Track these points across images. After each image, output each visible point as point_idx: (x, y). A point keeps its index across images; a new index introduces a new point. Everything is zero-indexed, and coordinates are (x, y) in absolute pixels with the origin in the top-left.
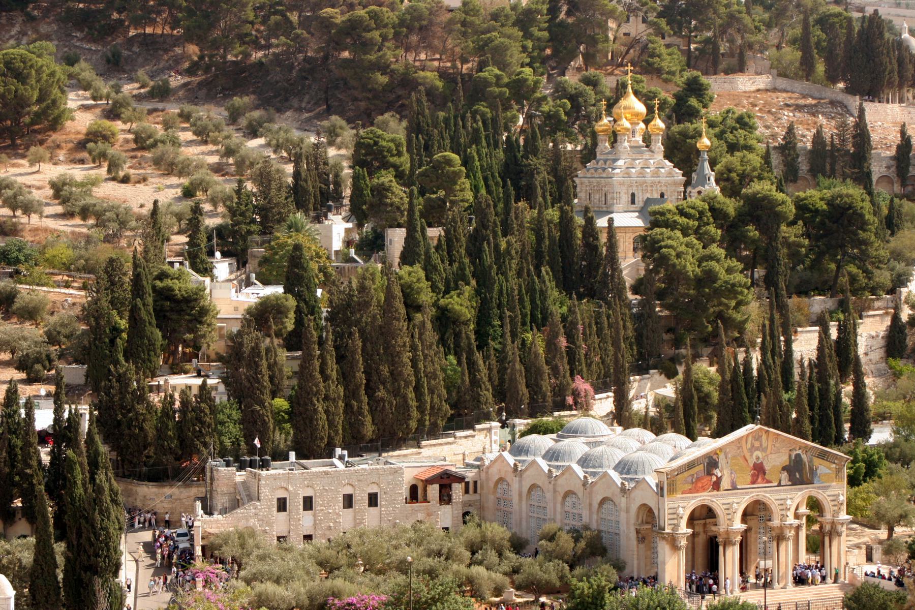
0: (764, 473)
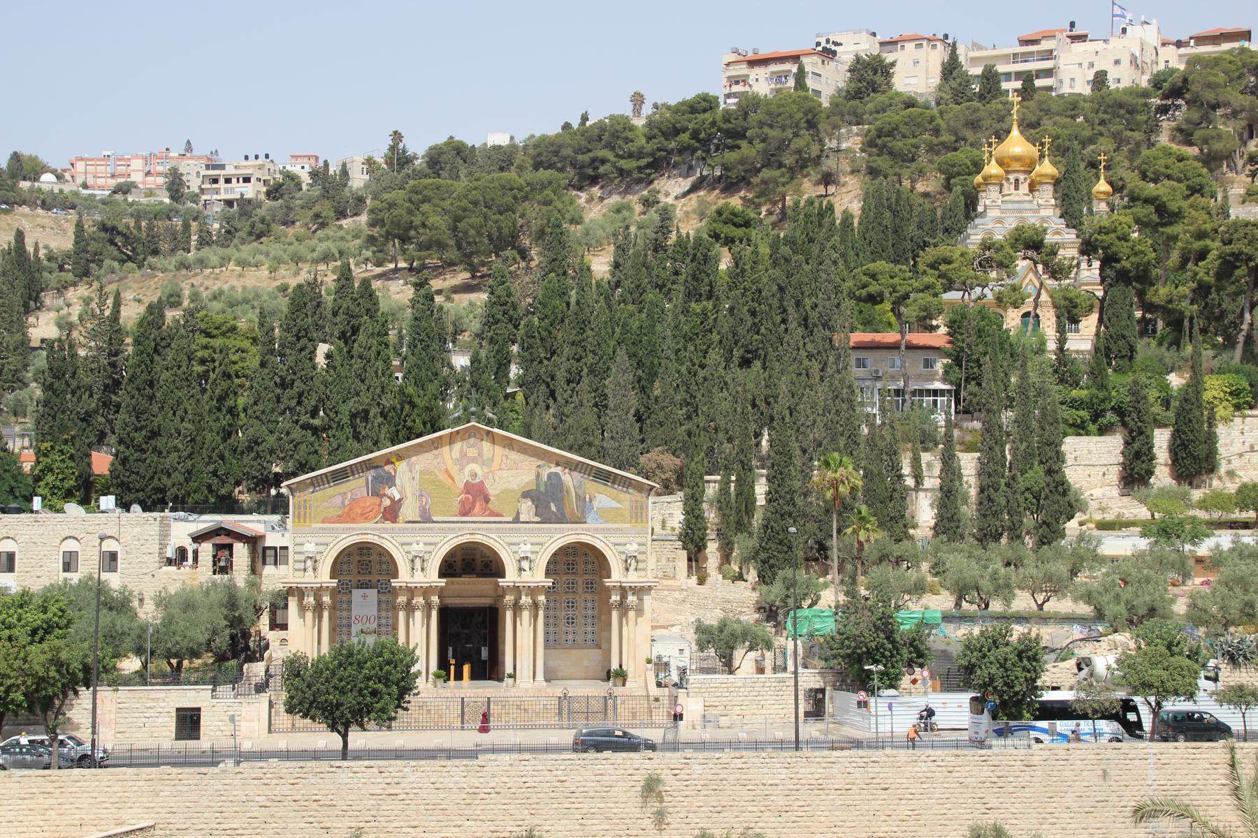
0: (487, 500)
